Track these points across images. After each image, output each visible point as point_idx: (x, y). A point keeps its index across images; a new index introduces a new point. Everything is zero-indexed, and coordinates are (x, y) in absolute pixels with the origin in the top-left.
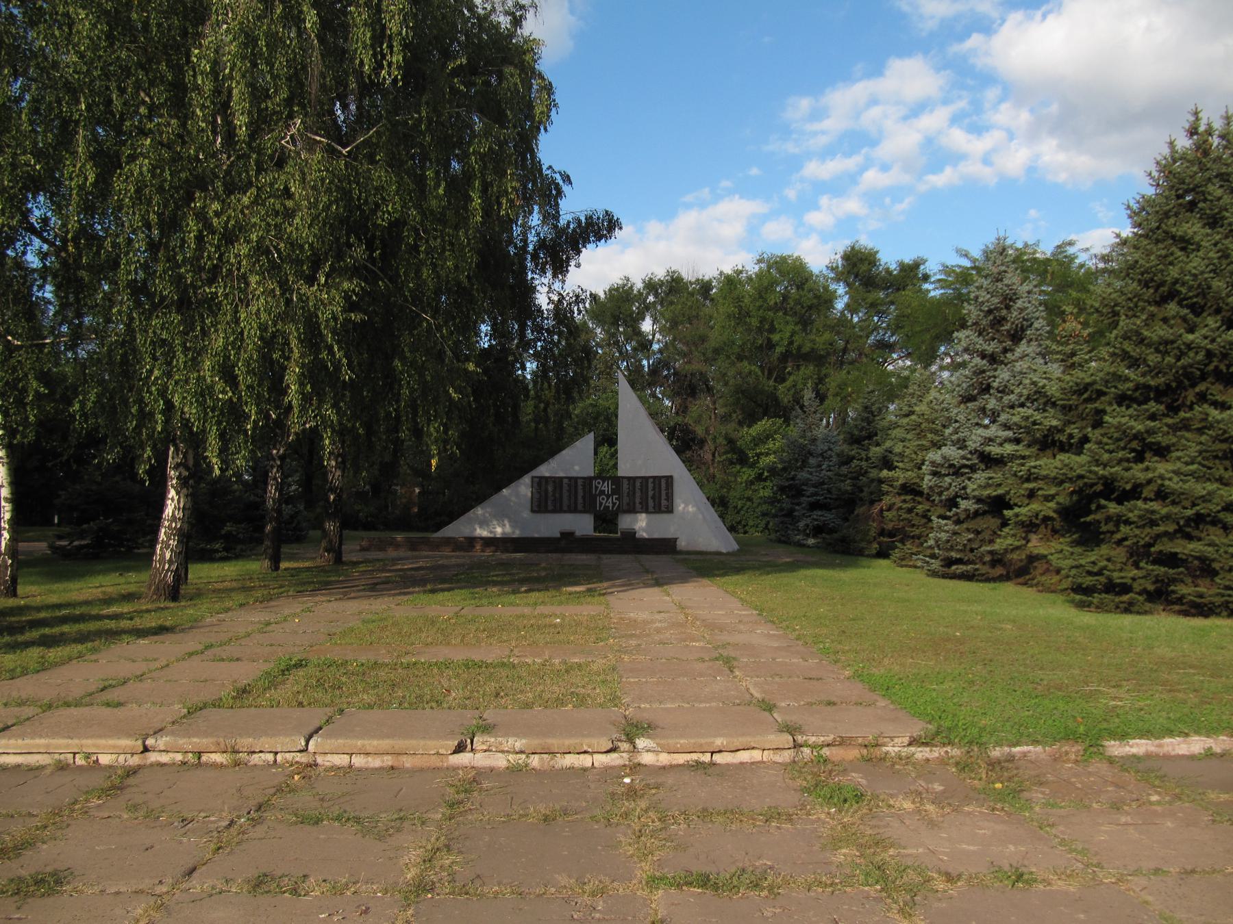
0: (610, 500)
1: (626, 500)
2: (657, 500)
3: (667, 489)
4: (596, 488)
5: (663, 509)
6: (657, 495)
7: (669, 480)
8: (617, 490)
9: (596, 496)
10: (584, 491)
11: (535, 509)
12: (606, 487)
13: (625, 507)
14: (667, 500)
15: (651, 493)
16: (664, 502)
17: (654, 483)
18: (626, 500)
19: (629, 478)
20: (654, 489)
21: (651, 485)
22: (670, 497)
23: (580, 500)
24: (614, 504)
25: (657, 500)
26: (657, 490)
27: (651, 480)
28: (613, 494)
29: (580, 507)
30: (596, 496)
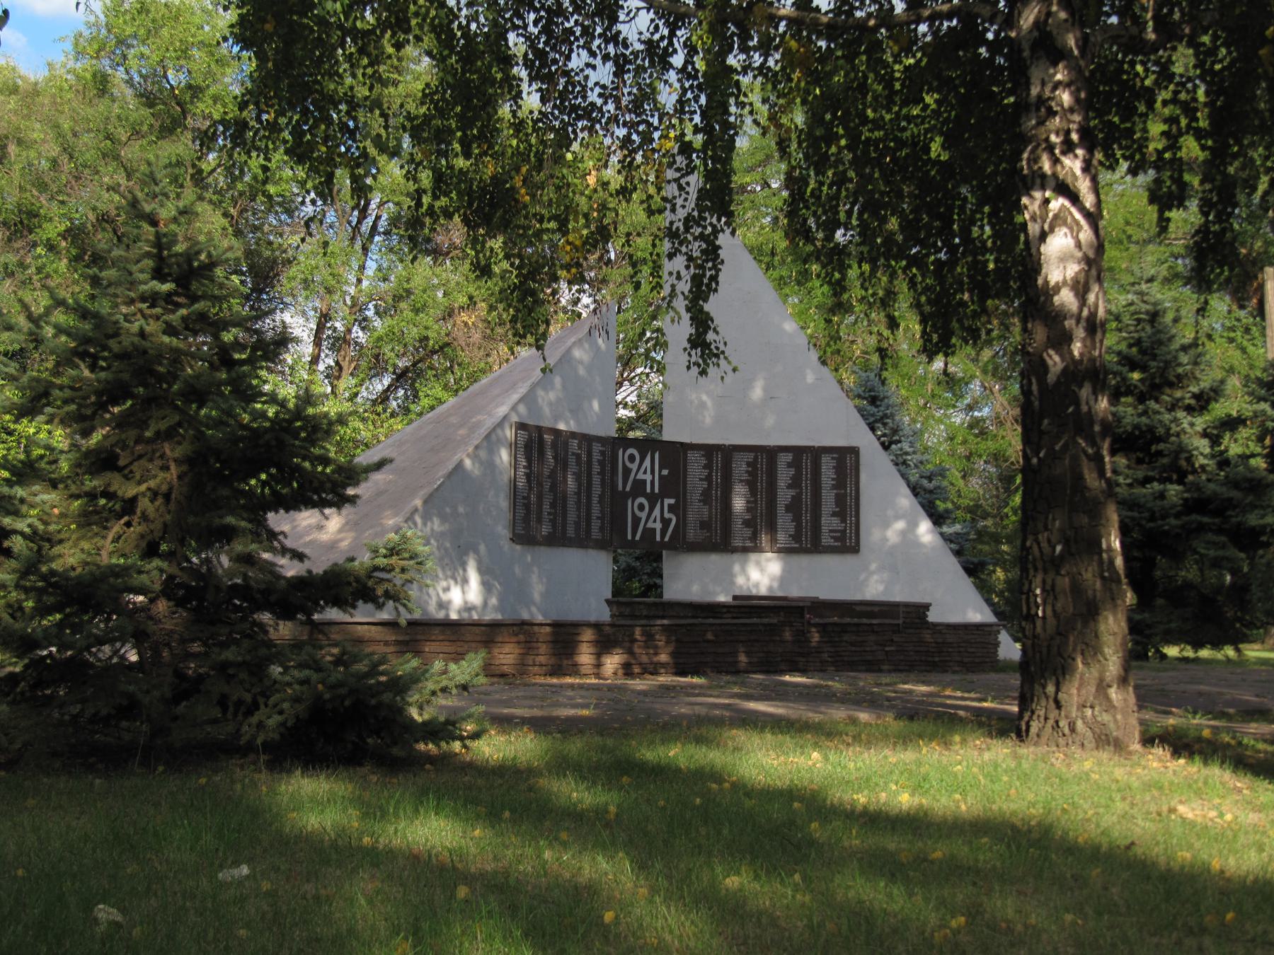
0: (657, 512)
1: (697, 511)
2: (806, 517)
3: (840, 483)
4: (627, 471)
5: (826, 540)
6: (807, 498)
7: (854, 451)
8: (673, 485)
9: (625, 496)
10: (603, 481)
11: (520, 531)
12: (648, 471)
13: (692, 534)
14: (841, 514)
15: (784, 495)
16: (829, 523)
17: (796, 464)
18: (697, 511)
19: (709, 450)
20: (795, 483)
21: (784, 475)
22: (848, 506)
23: (596, 511)
24: (666, 523)
25: (806, 517)
26: (806, 484)
27: (784, 458)
28: (664, 494)
29: (596, 534)
30: (625, 496)
